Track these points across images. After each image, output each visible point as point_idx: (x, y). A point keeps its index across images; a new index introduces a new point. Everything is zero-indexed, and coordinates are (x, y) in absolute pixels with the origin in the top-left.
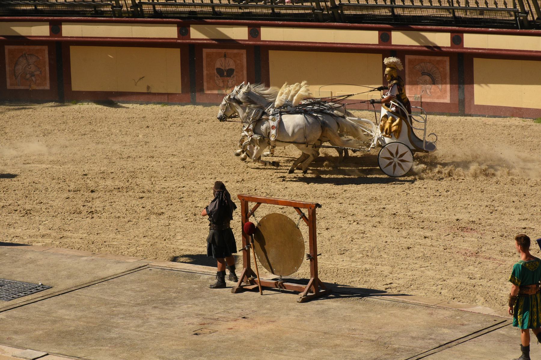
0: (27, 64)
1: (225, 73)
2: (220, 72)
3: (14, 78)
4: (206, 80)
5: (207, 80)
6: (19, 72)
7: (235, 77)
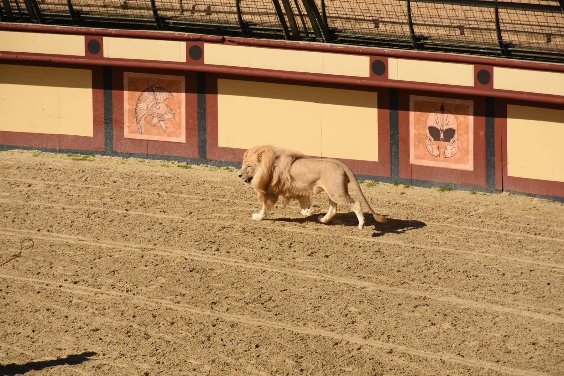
0: (154, 102)
1: (442, 136)
2: (434, 132)
3: (135, 122)
4: (413, 144)
5: (415, 143)
6: (143, 113)
7: (457, 142)
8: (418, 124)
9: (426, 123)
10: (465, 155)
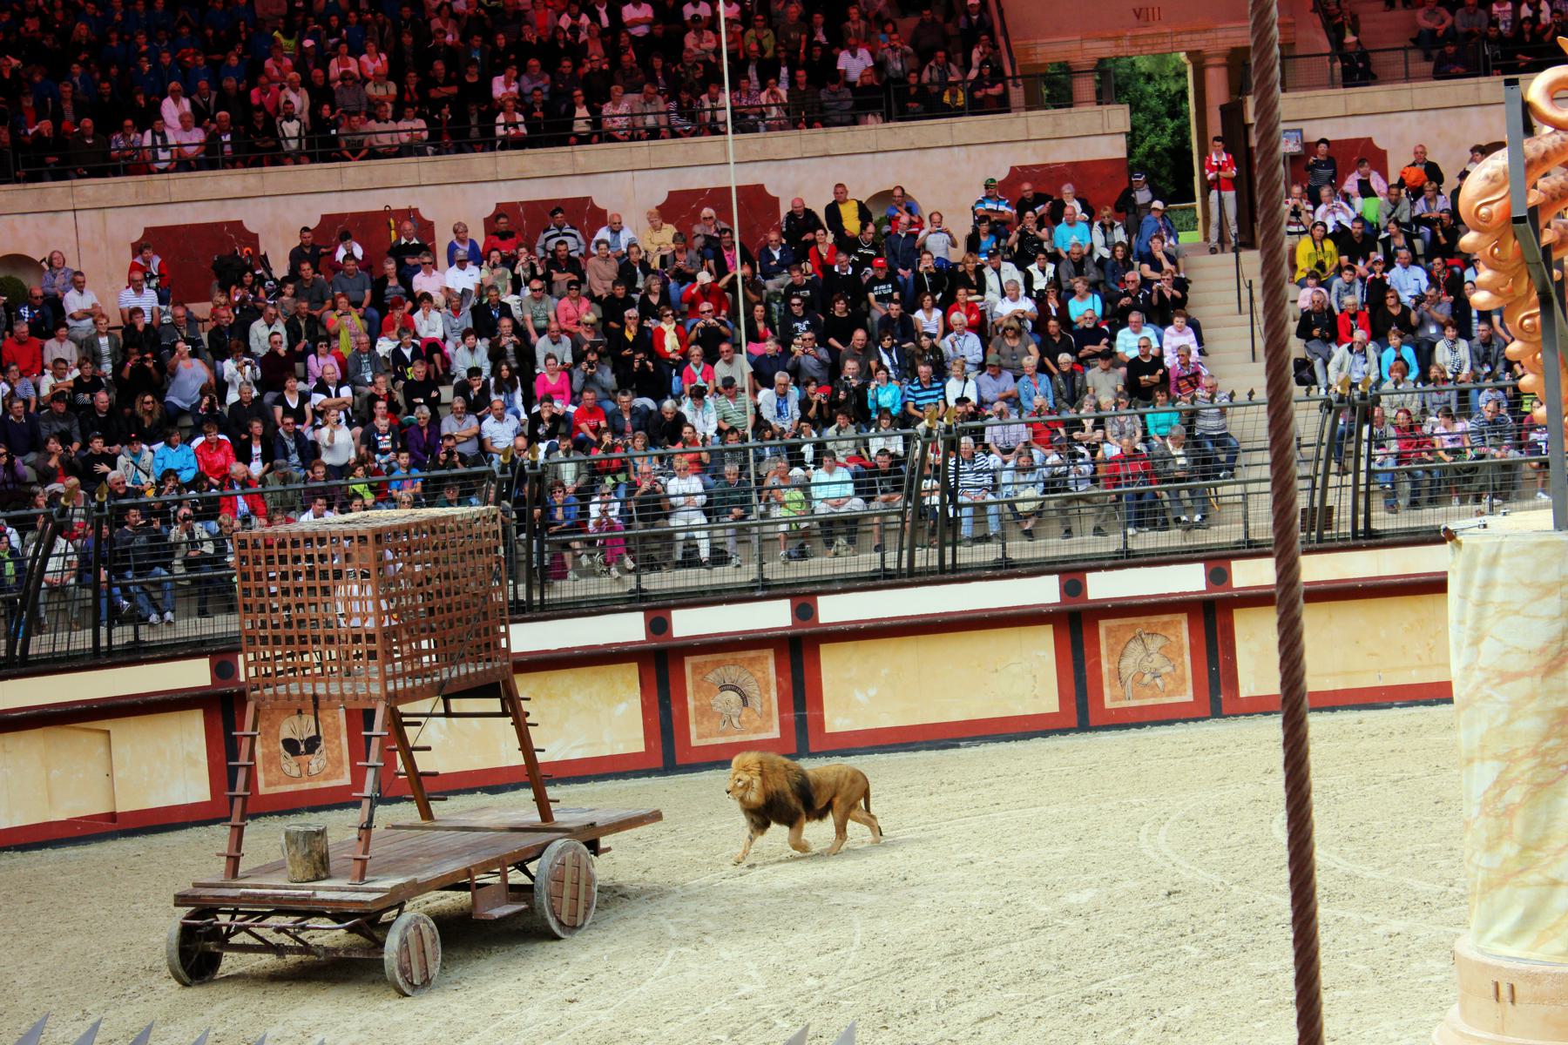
1: (302, 748)
2: (291, 746)
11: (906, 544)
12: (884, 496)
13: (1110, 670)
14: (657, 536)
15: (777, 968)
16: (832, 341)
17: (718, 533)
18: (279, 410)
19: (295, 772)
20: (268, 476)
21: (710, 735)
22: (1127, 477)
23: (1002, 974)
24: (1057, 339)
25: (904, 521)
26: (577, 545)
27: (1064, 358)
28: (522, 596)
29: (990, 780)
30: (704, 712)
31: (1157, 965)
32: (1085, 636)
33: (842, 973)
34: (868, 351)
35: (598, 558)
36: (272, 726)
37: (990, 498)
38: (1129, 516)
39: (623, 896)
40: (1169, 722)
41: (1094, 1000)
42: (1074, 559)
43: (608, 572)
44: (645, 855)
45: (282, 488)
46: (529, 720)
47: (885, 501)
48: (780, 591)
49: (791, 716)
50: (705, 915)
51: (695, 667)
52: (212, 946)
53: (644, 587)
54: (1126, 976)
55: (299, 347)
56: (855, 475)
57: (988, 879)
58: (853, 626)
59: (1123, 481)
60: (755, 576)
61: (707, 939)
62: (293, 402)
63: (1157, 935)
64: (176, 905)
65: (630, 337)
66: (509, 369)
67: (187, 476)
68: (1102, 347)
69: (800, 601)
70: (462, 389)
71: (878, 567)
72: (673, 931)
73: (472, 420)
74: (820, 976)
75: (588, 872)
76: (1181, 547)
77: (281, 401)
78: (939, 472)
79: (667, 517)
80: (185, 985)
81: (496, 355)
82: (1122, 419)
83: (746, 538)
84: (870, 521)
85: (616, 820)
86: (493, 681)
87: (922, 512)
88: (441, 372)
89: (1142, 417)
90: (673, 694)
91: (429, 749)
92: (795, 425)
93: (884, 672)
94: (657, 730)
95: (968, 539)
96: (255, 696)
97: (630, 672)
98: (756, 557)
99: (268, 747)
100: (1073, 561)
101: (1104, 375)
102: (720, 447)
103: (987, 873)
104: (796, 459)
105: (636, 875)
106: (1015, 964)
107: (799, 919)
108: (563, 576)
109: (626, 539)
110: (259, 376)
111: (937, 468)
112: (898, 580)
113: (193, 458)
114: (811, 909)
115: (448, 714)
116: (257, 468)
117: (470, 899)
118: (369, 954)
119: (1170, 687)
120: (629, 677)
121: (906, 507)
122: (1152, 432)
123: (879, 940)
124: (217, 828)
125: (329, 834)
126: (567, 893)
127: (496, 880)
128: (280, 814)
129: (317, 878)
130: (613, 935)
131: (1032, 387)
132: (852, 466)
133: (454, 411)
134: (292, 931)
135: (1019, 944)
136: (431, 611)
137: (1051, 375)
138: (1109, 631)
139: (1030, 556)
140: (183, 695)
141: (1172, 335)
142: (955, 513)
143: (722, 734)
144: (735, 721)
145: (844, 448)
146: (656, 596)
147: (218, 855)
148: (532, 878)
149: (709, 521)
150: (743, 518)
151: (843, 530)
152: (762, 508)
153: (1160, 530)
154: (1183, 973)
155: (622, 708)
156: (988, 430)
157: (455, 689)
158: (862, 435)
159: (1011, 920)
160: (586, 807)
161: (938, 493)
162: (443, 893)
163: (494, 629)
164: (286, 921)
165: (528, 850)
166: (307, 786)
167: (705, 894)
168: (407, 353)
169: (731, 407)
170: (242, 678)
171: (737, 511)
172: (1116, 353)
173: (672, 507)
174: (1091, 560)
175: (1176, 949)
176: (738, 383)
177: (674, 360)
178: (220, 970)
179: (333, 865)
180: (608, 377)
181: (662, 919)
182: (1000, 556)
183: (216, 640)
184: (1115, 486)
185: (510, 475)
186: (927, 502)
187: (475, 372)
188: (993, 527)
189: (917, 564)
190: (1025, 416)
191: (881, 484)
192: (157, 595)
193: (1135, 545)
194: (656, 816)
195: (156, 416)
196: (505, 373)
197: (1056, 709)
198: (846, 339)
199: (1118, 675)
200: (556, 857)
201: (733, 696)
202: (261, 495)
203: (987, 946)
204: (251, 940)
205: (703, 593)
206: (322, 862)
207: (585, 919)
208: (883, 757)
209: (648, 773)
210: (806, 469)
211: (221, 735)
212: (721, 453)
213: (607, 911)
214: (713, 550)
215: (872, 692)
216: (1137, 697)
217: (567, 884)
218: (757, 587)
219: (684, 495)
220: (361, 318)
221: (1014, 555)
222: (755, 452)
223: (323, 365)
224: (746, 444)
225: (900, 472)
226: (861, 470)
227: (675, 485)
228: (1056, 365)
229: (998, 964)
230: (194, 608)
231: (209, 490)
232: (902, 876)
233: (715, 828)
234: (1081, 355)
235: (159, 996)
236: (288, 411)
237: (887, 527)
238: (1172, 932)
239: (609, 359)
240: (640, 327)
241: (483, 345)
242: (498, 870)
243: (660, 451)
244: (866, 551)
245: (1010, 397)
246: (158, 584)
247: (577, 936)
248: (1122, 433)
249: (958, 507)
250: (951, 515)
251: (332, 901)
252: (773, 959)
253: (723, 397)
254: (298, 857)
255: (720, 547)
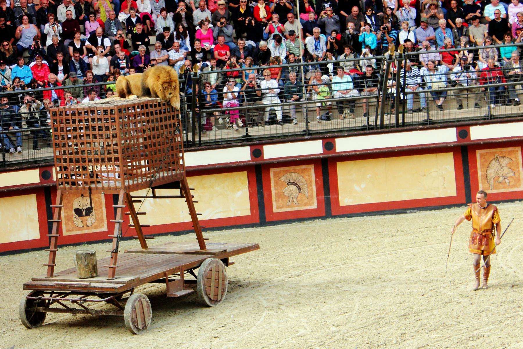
1: (84, 213)
2: (78, 212)
8: (66, 209)
9: (72, 207)
10: (101, 222)
11: (379, 112)
12: (369, 89)
13: (482, 175)
14: (257, 109)
15: (317, 322)
16: (342, 12)
17: (286, 107)
18: (71, 49)
19: (81, 225)
20: (66, 80)
21: (283, 207)
22: (490, 79)
23: (429, 325)
24: (455, 10)
25: (378, 101)
26: (217, 114)
27: (459, 20)
28: (190, 139)
29: (422, 230)
30: (280, 196)
31: (507, 322)
32: (469, 158)
33: (349, 324)
34: (360, 17)
35: (227, 120)
36: (69, 202)
37: (421, 90)
38: (491, 98)
39: (240, 286)
40: (512, 201)
41: (475, 339)
42: (464, 120)
43: (232, 127)
44: (251, 266)
45: (73, 86)
46: (194, 199)
47: (369, 91)
48: (317, 136)
49: (322, 198)
50: (281, 296)
51: (275, 174)
52: (41, 309)
53: (250, 134)
54: (491, 327)
55: (81, 18)
56: (354, 79)
57: (421, 278)
58: (353, 153)
59: (488, 81)
60: (305, 129)
61: (282, 307)
62: (78, 45)
63: (506, 307)
64: (24, 289)
65: (242, 11)
66: (183, 27)
67: (28, 81)
68: (478, 14)
69: (327, 140)
70: (160, 38)
71: (366, 124)
72: (265, 303)
73: (165, 52)
74: (338, 326)
75: (223, 274)
76: (518, 114)
77: (72, 44)
78: (396, 77)
79: (261, 100)
80: (29, 328)
81: (177, 19)
82: (488, 50)
83: (300, 110)
84: (361, 101)
85: (237, 249)
86: (176, 180)
87: (387, 97)
88: (150, 29)
89: (498, 49)
90: (264, 187)
91: (145, 214)
92: (324, 54)
93: (369, 176)
94: (256, 204)
95: (410, 110)
96: (60, 188)
97: (243, 176)
98: (305, 119)
99: (67, 213)
100: (463, 121)
101: (476, 28)
102: (287, 65)
103: (421, 275)
104: (325, 71)
105: (247, 276)
106: (435, 320)
107: (327, 298)
108: (210, 129)
109: (240, 111)
110: (61, 32)
111: (395, 74)
112: (376, 131)
113: (30, 72)
114: (333, 292)
115: (154, 197)
116: (61, 77)
117: (166, 287)
118: (117, 313)
119: (512, 183)
120: (242, 178)
121: (379, 94)
122: (503, 56)
123: (367, 308)
124: (43, 252)
125: (97, 255)
126: (213, 284)
127: (178, 278)
128: (74, 245)
129: (92, 276)
130: (236, 305)
131: (443, 35)
132: (352, 74)
133: (156, 48)
134: (79, 302)
135: (437, 311)
136: (146, 147)
137: (451, 28)
138: (481, 155)
139: (442, 118)
140: (26, 187)
141: (512, 7)
142: (404, 97)
143: (289, 206)
144: (295, 200)
145: (348, 66)
146: (256, 139)
147: (44, 265)
148: (196, 277)
149: (282, 102)
150: (298, 100)
151: (348, 106)
152: (308, 95)
153: (507, 105)
154: (520, 326)
155: (239, 194)
156: (421, 56)
157: (158, 185)
158: (357, 59)
159: (433, 299)
160: (222, 242)
161: (395, 87)
162: (152, 284)
163: (176, 155)
164: (77, 297)
165: (194, 263)
166: (86, 232)
167: (281, 285)
168: (134, 20)
169: (292, 45)
170: (55, 179)
171: (295, 97)
172: (484, 17)
173: (263, 94)
174: (473, 120)
175: (516, 314)
176: (297, 34)
177: (264, 22)
178: (45, 321)
179: (99, 270)
180: (230, 30)
181: (260, 297)
182: (426, 118)
183: (42, 161)
184: (484, 83)
185: (184, 79)
186: (389, 91)
187: (167, 29)
188: (423, 104)
189: (385, 123)
190: (438, 48)
191: (367, 83)
192: (13, 139)
193: (494, 113)
194: (257, 247)
195: (12, 52)
196: (181, 29)
197: (455, 195)
198: (349, 12)
199: (486, 177)
200: (207, 267)
201: (294, 188)
202: (63, 90)
203: (421, 311)
204: (60, 307)
205: (279, 137)
206: (94, 269)
207: (222, 297)
208: (368, 218)
209: (253, 226)
210: (329, 76)
211: (44, 207)
212: (287, 68)
213: (233, 293)
214: (284, 116)
215: (363, 186)
216: (495, 188)
217: (213, 280)
218: (305, 134)
219: (269, 88)
220: (111, 3)
221: (433, 118)
222: (304, 68)
223: (92, 26)
224: (300, 64)
225: (377, 77)
226: (357, 76)
227: (264, 84)
228: (455, 24)
229: (426, 321)
230: (31, 145)
231: (37, 87)
232: (378, 277)
233: (285, 253)
234: (467, 18)
235: (16, 333)
236: (75, 49)
237: (370, 104)
238: (514, 305)
239: (232, 22)
240: (247, 6)
241: (170, 16)
242: (179, 273)
243: (257, 67)
244: (360, 116)
245: (432, 39)
246: (14, 134)
247: (218, 305)
248: (488, 57)
249: (405, 94)
250: (402, 98)
251: (99, 288)
252: (314, 317)
253: (289, 40)
254: (82, 266)
255: (287, 114)
